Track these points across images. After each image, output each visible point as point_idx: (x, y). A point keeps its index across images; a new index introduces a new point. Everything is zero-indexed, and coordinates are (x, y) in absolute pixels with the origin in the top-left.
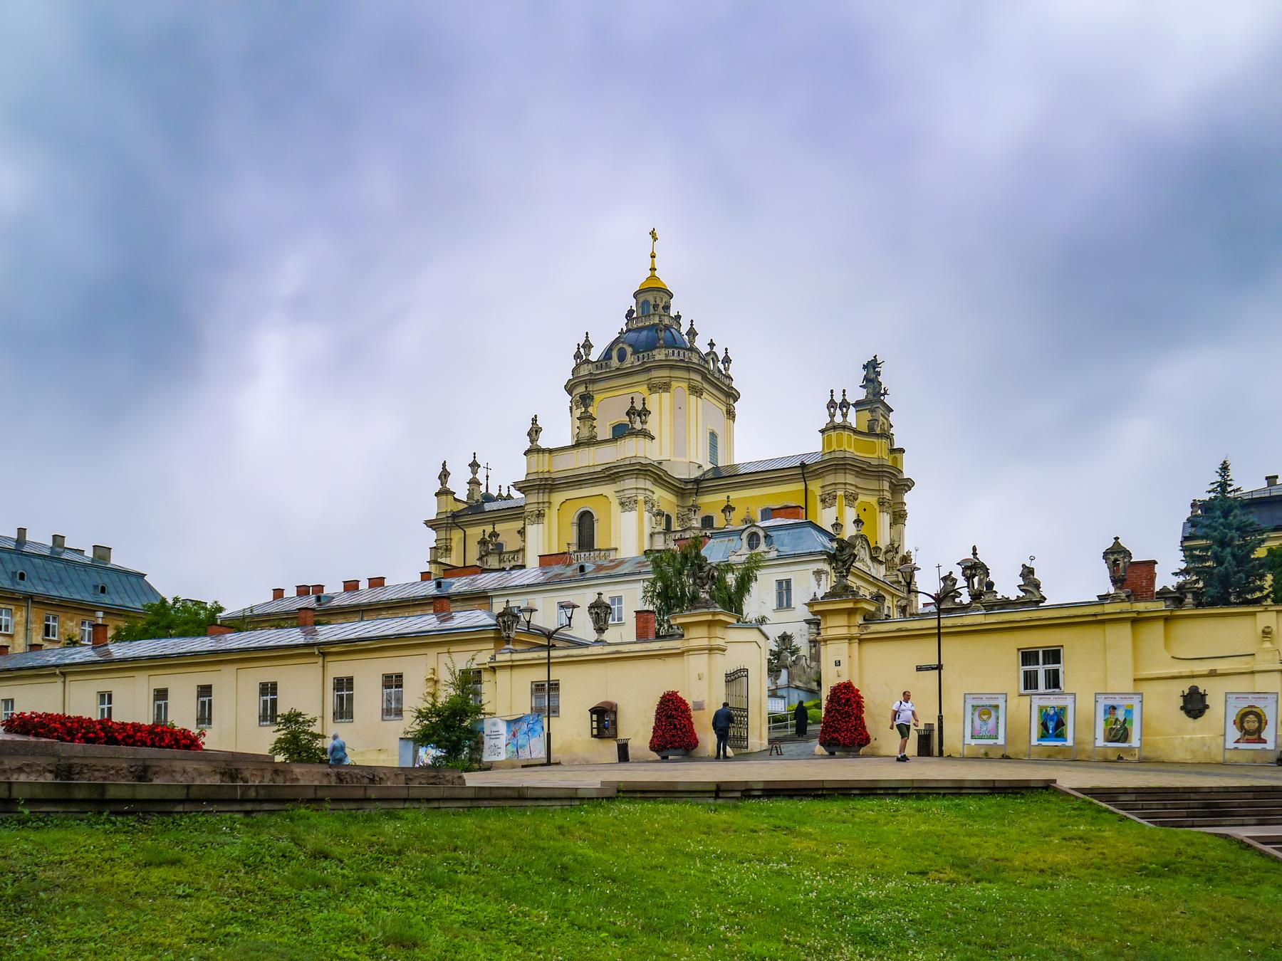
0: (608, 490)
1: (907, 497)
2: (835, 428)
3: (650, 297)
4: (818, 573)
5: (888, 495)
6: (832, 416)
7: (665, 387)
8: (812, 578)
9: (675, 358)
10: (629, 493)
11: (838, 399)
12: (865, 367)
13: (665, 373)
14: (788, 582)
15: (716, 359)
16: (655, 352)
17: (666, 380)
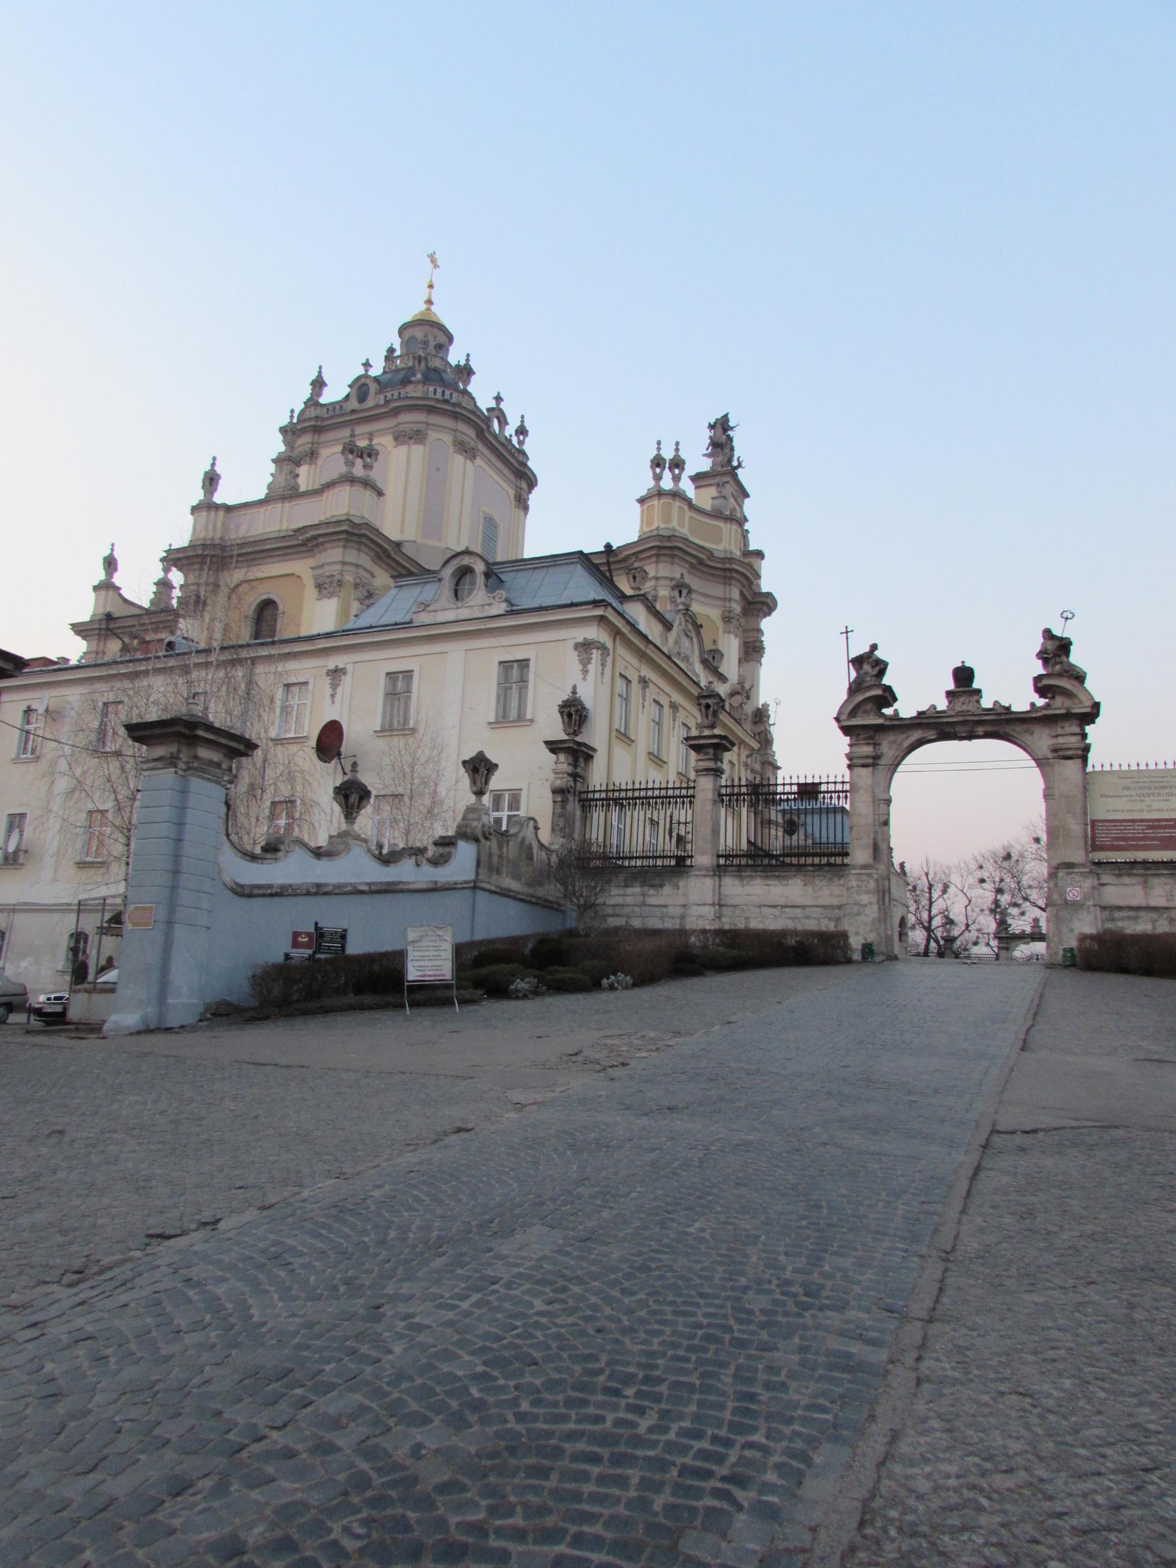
0: (302, 567)
1: (766, 624)
2: (660, 493)
3: (419, 333)
4: (585, 647)
5: (737, 608)
6: (658, 478)
7: (417, 436)
8: (573, 657)
9: (439, 396)
10: (328, 571)
11: (668, 454)
12: (711, 427)
13: (421, 417)
14: (524, 664)
15: (503, 421)
16: (409, 388)
17: (421, 427)
